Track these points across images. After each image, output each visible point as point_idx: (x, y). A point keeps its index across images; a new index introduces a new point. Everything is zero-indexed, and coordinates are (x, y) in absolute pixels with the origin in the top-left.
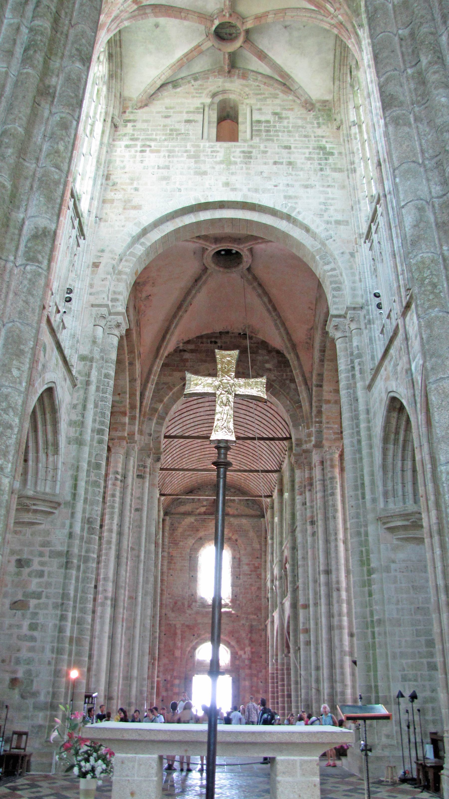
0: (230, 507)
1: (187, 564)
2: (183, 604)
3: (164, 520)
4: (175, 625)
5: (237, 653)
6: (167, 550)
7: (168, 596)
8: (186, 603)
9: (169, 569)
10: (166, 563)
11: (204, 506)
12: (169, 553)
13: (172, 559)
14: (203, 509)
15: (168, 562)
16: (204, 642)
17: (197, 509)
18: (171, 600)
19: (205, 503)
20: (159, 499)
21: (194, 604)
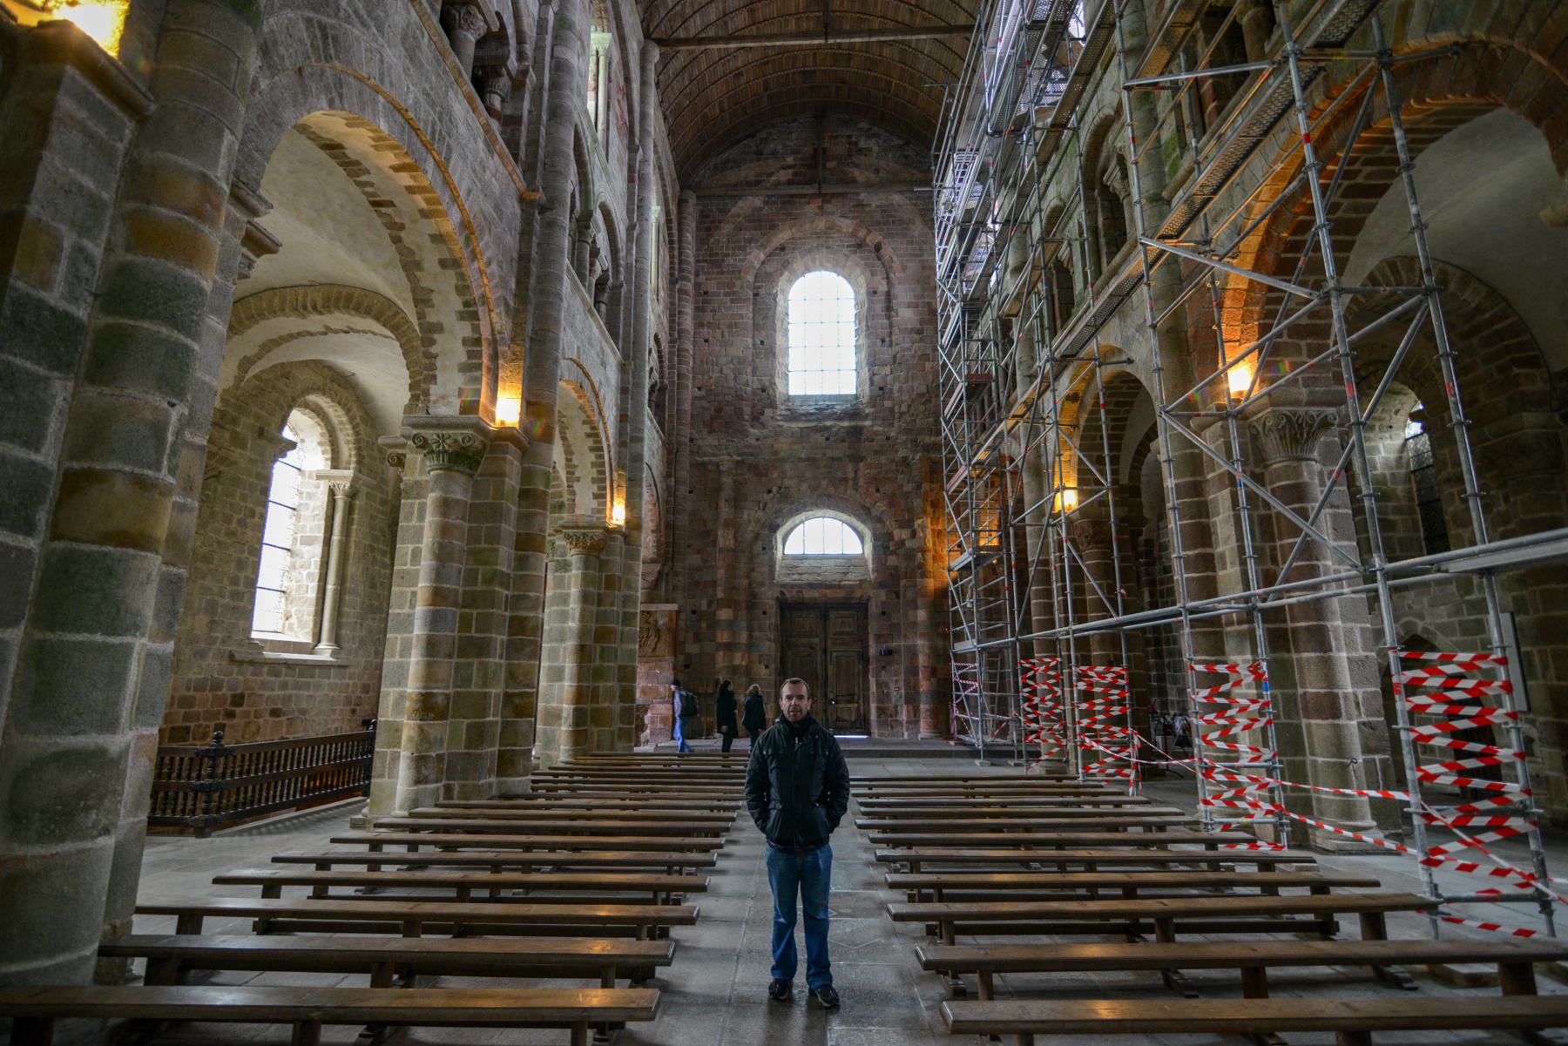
0: (857, 166)
1: (747, 311)
2: (739, 413)
3: (681, 203)
4: (718, 465)
5: (890, 536)
6: (692, 277)
7: (698, 393)
8: (747, 410)
9: (699, 325)
10: (689, 309)
11: (784, 168)
12: (697, 285)
13: (705, 302)
14: (784, 176)
15: (697, 309)
16: (797, 512)
17: (771, 174)
18: (704, 403)
19: (790, 160)
20: (644, 55)
21: (768, 412)
